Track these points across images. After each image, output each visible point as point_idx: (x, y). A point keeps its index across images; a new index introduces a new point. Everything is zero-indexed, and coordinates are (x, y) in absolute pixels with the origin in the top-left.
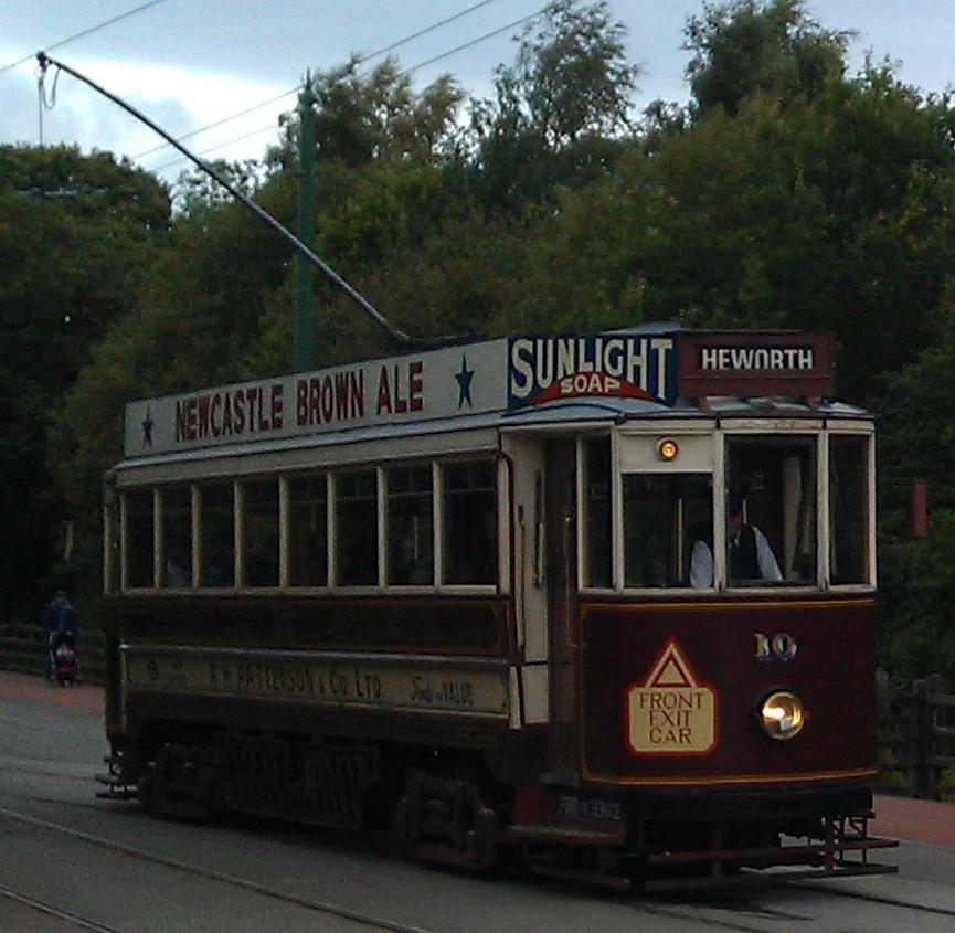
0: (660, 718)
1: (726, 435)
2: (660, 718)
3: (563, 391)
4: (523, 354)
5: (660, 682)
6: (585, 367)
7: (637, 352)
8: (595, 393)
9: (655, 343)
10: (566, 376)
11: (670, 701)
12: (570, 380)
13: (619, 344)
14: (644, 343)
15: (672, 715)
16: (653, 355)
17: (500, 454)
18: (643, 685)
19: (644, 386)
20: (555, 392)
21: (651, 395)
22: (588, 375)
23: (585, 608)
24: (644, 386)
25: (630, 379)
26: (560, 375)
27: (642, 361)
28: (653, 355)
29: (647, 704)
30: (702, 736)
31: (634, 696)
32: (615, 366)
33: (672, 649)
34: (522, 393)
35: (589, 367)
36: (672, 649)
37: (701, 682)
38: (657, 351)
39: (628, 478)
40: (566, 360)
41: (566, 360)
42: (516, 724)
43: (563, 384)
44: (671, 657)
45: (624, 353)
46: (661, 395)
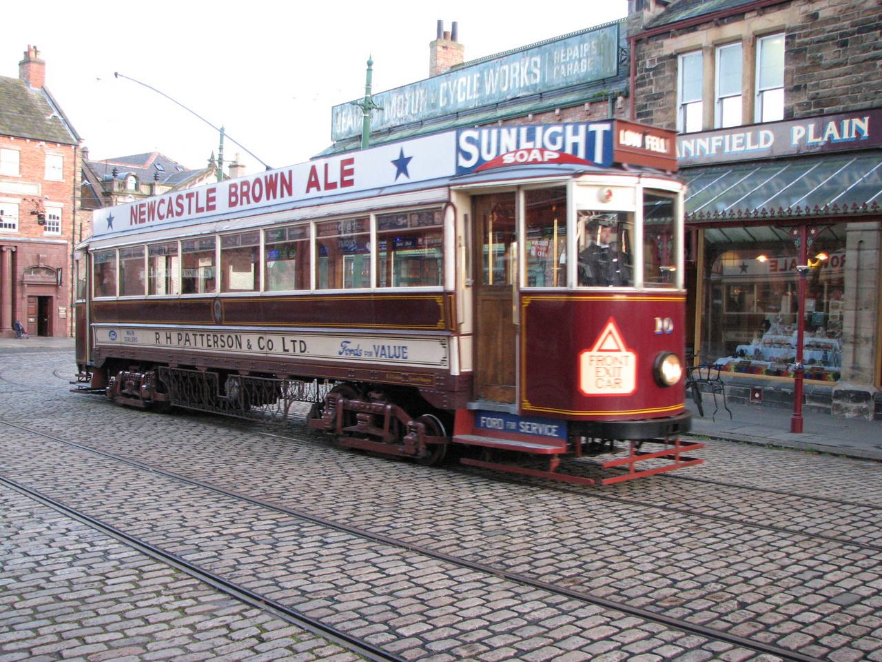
0: (602, 373)
2: (602, 373)
3: (505, 162)
5: (604, 348)
6: (525, 145)
7: (575, 133)
8: (535, 162)
10: (508, 152)
11: (609, 361)
12: (513, 154)
17: (449, 203)
22: (529, 151)
23: (527, 301)
24: (581, 154)
25: (569, 151)
26: (503, 151)
27: (581, 139)
31: (586, 358)
32: (553, 142)
33: (611, 327)
34: (464, 163)
35: (530, 145)
36: (611, 327)
37: (630, 346)
38: (593, 133)
43: (505, 157)
44: (610, 333)
45: (563, 134)
46: (598, 158)
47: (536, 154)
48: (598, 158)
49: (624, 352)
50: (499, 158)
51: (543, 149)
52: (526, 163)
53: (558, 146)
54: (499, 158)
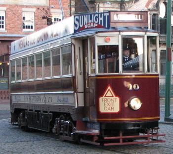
0: (107, 105)
1: (122, 36)
2: (107, 105)
4: (77, 19)
6: (90, 21)
8: (92, 28)
9: (105, 14)
10: (86, 24)
11: (109, 100)
13: (97, 15)
14: (103, 15)
15: (110, 104)
16: (104, 17)
18: (102, 96)
19: (103, 25)
20: (83, 28)
21: (104, 27)
22: (91, 23)
24: (103, 25)
25: (100, 23)
27: (102, 19)
28: (104, 17)
29: (104, 101)
30: (117, 109)
31: (101, 99)
32: (96, 20)
33: (109, 88)
35: (90, 21)
36: (109, 88)
37: (117, 95)
39: (99, 47)
40: (86, 20)
41: (86, 20)
42: (76, 107)
44: (109, 90)
46: (106, 26)
47: (92, 25)
48: (106, 26)
49: (115, 97)
50: (84, 26)
51: (94, 23)
52: (90, 28)
53: (97, 22)
54: (84, 26)
